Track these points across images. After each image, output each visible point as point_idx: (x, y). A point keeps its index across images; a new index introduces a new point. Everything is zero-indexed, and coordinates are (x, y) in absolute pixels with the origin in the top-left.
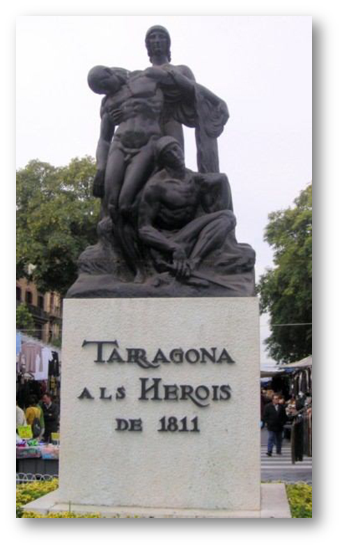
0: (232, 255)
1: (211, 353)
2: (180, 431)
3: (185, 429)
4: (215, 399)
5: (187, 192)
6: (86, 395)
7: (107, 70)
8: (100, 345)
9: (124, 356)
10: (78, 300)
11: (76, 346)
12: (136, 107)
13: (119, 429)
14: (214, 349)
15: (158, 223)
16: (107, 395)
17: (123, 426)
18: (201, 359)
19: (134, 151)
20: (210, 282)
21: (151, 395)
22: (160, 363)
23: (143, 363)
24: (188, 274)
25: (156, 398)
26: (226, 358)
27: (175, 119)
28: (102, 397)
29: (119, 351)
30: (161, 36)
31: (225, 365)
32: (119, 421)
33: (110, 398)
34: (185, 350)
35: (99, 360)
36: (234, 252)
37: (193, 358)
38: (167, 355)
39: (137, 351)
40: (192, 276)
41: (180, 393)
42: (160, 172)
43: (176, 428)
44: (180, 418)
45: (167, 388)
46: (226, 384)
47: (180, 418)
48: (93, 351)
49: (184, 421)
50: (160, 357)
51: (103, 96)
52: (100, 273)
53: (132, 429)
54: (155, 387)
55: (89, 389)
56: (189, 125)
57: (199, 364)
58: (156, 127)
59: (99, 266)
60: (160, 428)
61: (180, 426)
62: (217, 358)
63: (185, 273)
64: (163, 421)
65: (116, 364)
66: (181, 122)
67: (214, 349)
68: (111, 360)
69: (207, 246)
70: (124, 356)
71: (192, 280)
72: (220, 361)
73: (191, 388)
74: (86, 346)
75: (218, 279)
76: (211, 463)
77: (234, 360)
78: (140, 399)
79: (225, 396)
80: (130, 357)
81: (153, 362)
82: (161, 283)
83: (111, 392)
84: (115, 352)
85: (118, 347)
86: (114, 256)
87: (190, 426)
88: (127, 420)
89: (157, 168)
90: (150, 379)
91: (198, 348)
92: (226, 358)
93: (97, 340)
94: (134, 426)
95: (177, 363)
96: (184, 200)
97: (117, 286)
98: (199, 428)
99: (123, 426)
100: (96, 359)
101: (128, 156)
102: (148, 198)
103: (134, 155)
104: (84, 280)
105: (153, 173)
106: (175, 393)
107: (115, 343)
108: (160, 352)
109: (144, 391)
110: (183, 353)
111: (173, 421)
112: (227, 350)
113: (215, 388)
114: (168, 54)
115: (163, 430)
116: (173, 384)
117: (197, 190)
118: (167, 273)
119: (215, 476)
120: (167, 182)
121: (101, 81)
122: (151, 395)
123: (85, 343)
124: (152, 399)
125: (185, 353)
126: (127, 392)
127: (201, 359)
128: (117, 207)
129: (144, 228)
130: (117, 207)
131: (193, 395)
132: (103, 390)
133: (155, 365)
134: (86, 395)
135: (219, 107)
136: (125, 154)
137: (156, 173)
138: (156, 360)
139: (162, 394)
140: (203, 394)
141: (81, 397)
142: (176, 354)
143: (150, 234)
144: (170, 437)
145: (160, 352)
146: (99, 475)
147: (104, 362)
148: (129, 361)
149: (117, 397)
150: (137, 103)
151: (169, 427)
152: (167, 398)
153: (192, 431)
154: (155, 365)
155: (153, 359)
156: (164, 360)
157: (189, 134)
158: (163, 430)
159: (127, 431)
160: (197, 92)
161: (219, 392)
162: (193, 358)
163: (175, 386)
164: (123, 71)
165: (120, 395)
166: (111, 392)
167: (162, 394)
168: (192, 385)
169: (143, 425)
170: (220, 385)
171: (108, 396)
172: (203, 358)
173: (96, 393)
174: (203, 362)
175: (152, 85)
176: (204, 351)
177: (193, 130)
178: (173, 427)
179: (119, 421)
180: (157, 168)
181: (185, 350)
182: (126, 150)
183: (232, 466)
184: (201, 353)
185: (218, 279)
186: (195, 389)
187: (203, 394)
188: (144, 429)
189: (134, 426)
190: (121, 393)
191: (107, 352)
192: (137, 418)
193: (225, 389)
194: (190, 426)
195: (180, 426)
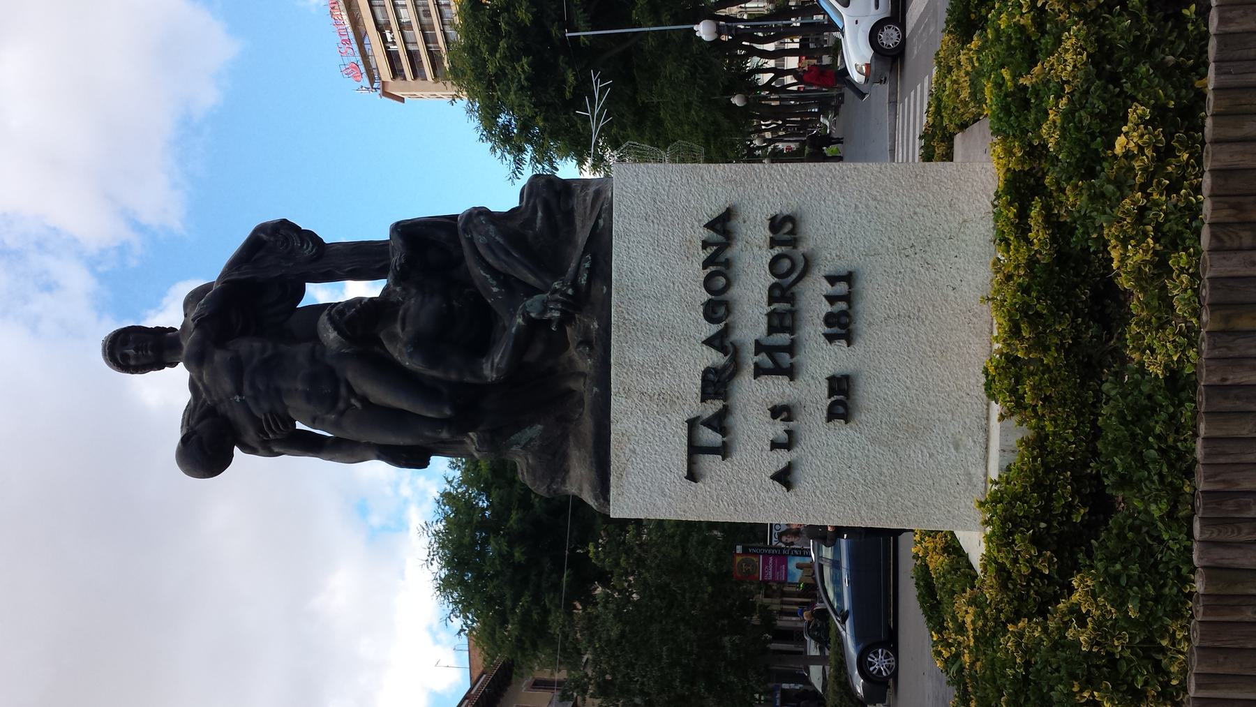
1: (711, 250)
2: (850, 307)
3: (847, 298)
6: (784, 477)
7: (185, 440)
8: (695, 450)
9: (714, 407)
10: (613, 492)
15: (482, 348)
16: (784, 437)
17: (841, 410)
19: (343, 391)
20: (584, 253)
21: (785, 358)
22: (727, 343)
23: (728, 373)
25: (791, 349)
29: (706, 416)
30: (125, 344)
32: (832, 415)
33: (790, 433)
34: (706, 296)
35: (723, 451)
36: (535, 212)
38: (714, 329)
43: (844, 313)
44: (826, 308)
45: (771, 330)
46: (767, 223)
47: (826, 308)
49: (831, 299)
51: (236, 450)
54: (771, 350)
55: (773, 471)
56: (301, 293)
58: (301, 351)
60: (843, 343)
61: (842, 305)
63: (568, 296)
64: (830, 338)
67: (705, 245)
70: (714, 407)
71: (583, 281)
73: (772, 288)
75: (582, 237)
76: (910, 252)
78: (792, 379)
79: (789, 226)
81: (725, 355)
82: (586, 342)
83: (778, 429)
84: (708, 423)
85: (698, 418)
87: (842, 288)
88: (829, 401)
89: (377, 349)
90: (756, 359)
91: (703, 274)
93: (685, 457)
94: (841, 387)
95: (729, 311)
98: (845, 273)
101: (353, 401)
104: (579, 483)
107: (692, 424)
108: (709, 342)
109: (778, 370)
110: (710, 301)
111: (829, 320)
113: (773, 243)
118: (568, 329)
120: (403, 329)
122: (785, 358)
123: (692, 476)
124: (792, 356)
125: (710, 296)
126: (778, 401)
133: (731, 349)
134: (784, 477)
138: (722, 349)
139: (782, 338)
140: (786, 264)
143: (496, 360)
144: (861, 325)
145: (709, 342)
146: (931, 455)
147: (724, 442)
149: (789, 419)
150: (253, 386)
151: (843, 326)
153: (850, 287)
154: (731, 349)
155: (721, 355)
157: (318, 293)
158: (849, 337)
159: (848, 403)
163: (769, 315)
164: (190, 412)
165: (785, 415)
166: (778, 429)
167: (782, 338)
168: (768, 284)
170: (768, 234)
171: (786, 436)
173: (782, 459)
174: (728, 263)
175: (219, 356)
176: (705, 265)
177: (310, 287)
178: (844, 320)
179: (832, 415)
180: (377, 349)
181: (706, 296)
182: (341, 405)
183: (915, 213)
184: (712, 268)
185: (582, 237)
187: (786, 264)
188: (845, 372)
189: (841, 387)
190: (781, 412)
191: (709, 436)
192: (825, 385)
193: (776, 224)
194: (842, 288)
195: (842, 305)
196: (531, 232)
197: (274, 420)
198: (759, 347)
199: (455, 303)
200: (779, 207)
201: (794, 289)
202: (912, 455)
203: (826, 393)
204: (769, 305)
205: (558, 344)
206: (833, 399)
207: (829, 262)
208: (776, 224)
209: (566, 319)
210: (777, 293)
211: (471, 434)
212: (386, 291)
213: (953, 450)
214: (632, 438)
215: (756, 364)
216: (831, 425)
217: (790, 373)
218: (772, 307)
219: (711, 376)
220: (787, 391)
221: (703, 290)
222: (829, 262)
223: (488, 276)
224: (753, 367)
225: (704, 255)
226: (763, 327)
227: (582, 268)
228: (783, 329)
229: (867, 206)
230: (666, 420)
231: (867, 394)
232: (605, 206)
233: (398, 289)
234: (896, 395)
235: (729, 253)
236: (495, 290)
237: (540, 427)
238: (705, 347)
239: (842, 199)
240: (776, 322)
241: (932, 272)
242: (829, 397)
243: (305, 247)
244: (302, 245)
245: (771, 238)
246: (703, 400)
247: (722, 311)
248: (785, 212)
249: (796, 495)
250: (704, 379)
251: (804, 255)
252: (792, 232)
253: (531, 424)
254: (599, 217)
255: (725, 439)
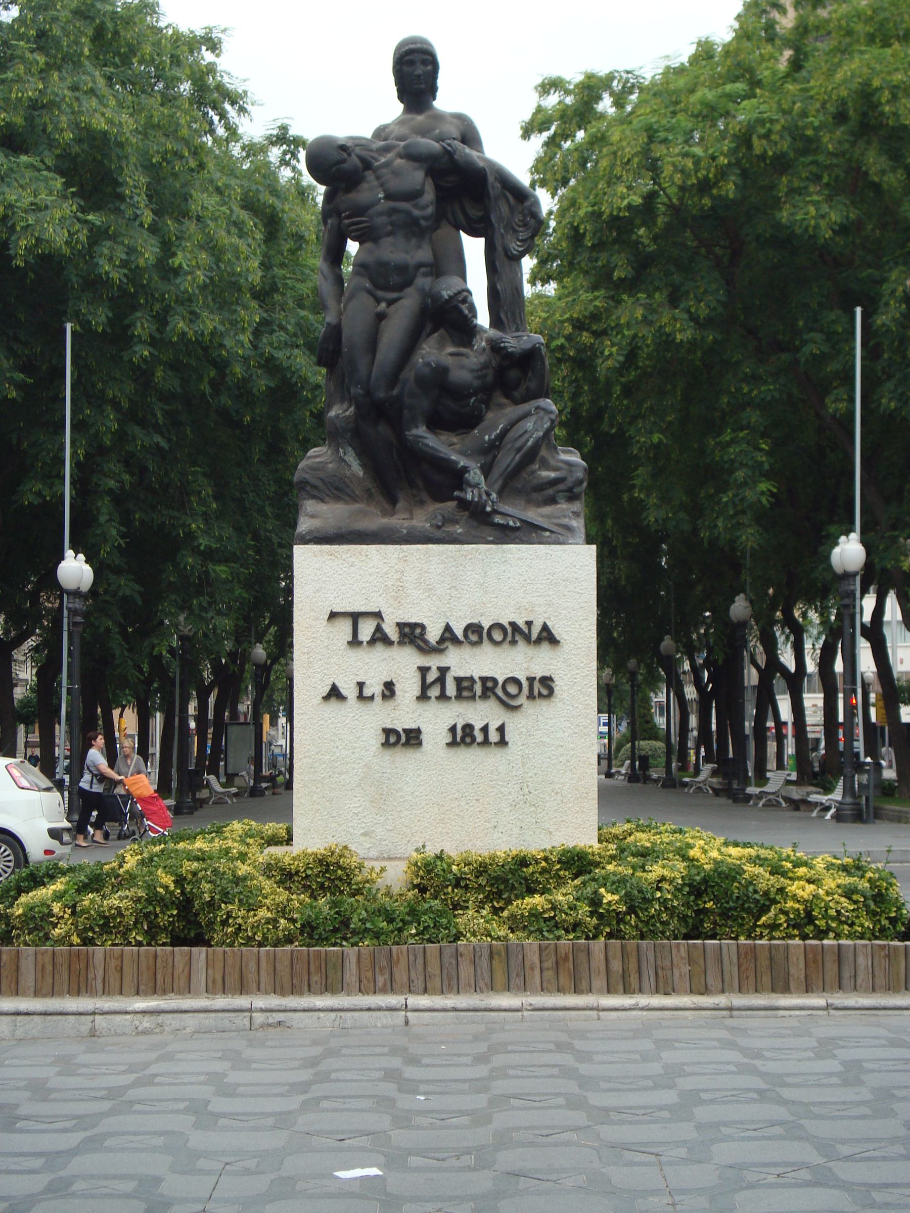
0: (553, 475)
3: (486, 742)
4: (531, 697)
5: (481, 370)
6: (334, 693)
8: (355, 617)
9: (392, 633)
11: (316, 619)
12: (394, 218)
13: (386, 744)
14: (529, 624)
16: (367, 692)
17: (392, 739)
18: (509, 638)
19: (394, 295)
20: (521, 520)
21: (434, 692)
22: (447, 644)
23: (421, 644)
24: (488, 509)
25: (443, 697)
26: (547, 637)
27: (450, 223)
28: (361, 697)
31: (545, 646)
32: (388, 732)
33: (372, 698)
34: (486, 625)
35: (355, 642)
36: (556, 469)
37: (497, 636)
38: (459, 633)
39: (414, 626)
40: (495, 512)
41: (478, 688)
42: (436, 335)
43: (474, 739)
44: (478, 725)
45: (459, 680)
46: (547, 674)
48: (345, 626)
49: (485, 729)
50: (448, 636)
52: (337, 499)
53: (407, 744)
54: (441, 680)
55: (337, 684)
56: (474, 233)
57: (506, 646)
59: (337, 489)
60: (449, 740)
61: (480, 738)
62: (534, 636)
63: (485, 507)
64: (453, 729)
65: (379, 647)
66: (458, 228)
67: (529, 624)
68: (372, 641)
69: (514, 463)
70: (392, 633)
71: (498, 519)
72: (539, 641)
73: (494, 680)
74: (333, 620)
75: (534, 515)
77: (558, 638)
78: (417, 698)
79: (545, 692)
80: (402, 635)
81: (437, 642)
83: (374, 688)
84: (379, 629)
85: (382, 619)
86: (356, 468)
87: (494, 737)
88: (400, 730)
90: (434, 668)
91: (505, 622)
92: (547, 637)
95: (474, 644)
96: (476, 383)
97: (377, 521)
98: (507, 739)
99: (392, 739)
100: (350, 639)
102: (420, 381)
103: (390, 303)
105: (424, 334)
106: (471, 689)
107: (378, 615)
108: (448, 628)
109: (425, 687)
110: (482, 628)
111: (468, 728)
112: (549, 624)
113: (531, 680)
114: (432, 90)
115: (453, 744)
116: (468, 675)
117: (494, 363)
119: (533, 809)
120: (451, 354)
121: (334, 169)
122: (434, 692)
123: (333, 615)
124: (437, 698)
125: (486, 628)
126: (398, 688)
127: (509, 638)
128: (368, 393)
129: (415, 432)
130: (368, 393)
131: (499, 691)
132: (361, 685)
134: (334, 693)
135: (527, 204)
136: (378, 301)
137: (429, 335)
138: (442, 640)
139: (451, 690)
140: (513, 690)
141: (327, 698)
142: (473, 632)
143: (426, 441)
145: (448, 628)
147: (362, 642)
148: (401, 643)
149: (384, 697)
150: (394, 211)
152: (459, 697)
154: (442, 647)
155: (438, 638)
156: (455, 640)
158: (453, 744)
160: (491, 179)
161: (537, 686)
162: (497, 636)
163: (471, 679)
165: (387, 693)
166: (374, 688)
167: (451, 690)
169: (424, 737)
171: (369, 695)
172: (513, 636)
174: (514, 642)
176: (512, 624)
177: (481, 241)
178: (468, 740)
179: (388, 732)
181: (486, 625)
182: (380, 294)
184: (509, 630)
185: (534, 515)
186: (501, 682)
187: (513, 690)
188: (424, 743)
190: (389, 689)
191: (366, 630)
192: (413, 726)
193: (547, 681)
194: (494, 737)
195: (480, 738)
196: (537, 466)
197: (364, 228)
198: (443, 671)
199: (472, 400)
200: (559, 685)
201: (493, 698)
202: (356, 799)
203: (407, 727)
204: (481, 678)
205: (440, 495)
206: (402, 732)
207: (516, 725)
208: (547, 681)
209: (464, 504)
210: (490, 684)
211: (352, 409)
212: (482, 328)
213: (362, 831)
214: (364, 564)
215: (428, 669)
216: (380, 731)
217: (423, 697)
218: (477, 680)
219: (418, 631)
220: (408, 695)
221: (491, 623)
222: (516, 725)
223: (498, 431)
224: (427, 665)
225: (521, 623)
226: (461, 674)
227: (509, 518)
228: (460, 689)
229: (562, 755)
230: (380, 593)
231: (404, 758)
232: (561, 538)
233: (484, 344)
234: (407, 783)
235: (521, 644)
236: (487, 438)
237: (361, 474)
238: (444, 624)
239: (567, 734)
240: (465, 684)
241: (508, 809)
242: (404, 730)
243: (519, 243)
244: (520, 241)
245: (534, 678)
246: (398, 624)
247: (474, 638)
248: (556, 689)
249: (319, 704)
250: (416, 625)
251: (520, 706)
252: (540, 695)
253: (363, 465)
254: (551, 532)
255: (365, 643)
